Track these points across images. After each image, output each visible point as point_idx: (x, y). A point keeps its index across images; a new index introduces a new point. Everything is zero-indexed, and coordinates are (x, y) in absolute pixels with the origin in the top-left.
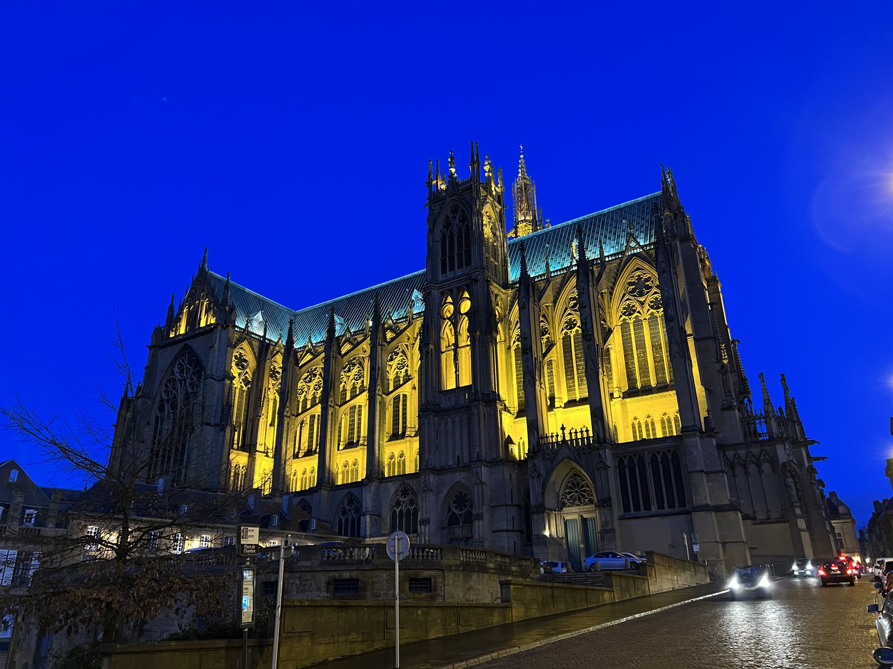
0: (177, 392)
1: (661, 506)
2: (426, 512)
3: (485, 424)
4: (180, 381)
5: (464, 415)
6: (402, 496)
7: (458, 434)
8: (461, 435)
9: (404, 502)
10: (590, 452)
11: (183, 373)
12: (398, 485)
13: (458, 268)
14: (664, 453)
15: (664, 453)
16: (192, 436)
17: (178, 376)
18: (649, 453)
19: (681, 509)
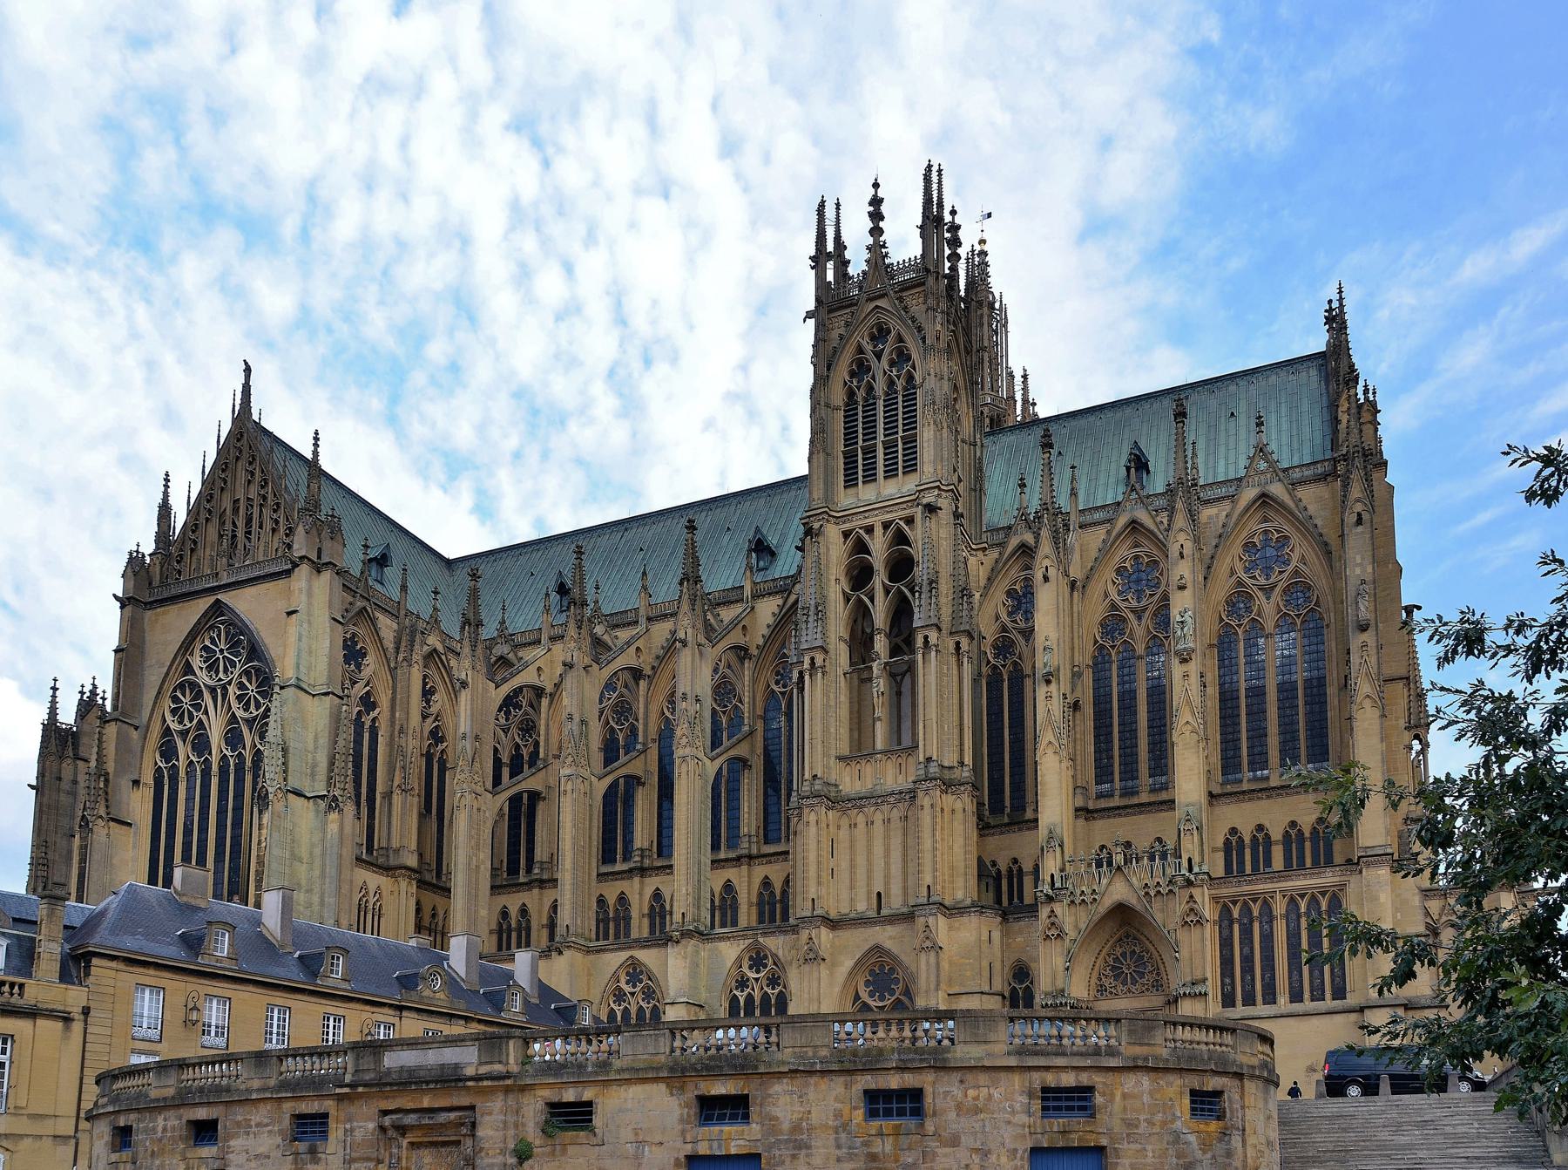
0: (206, 712)
1: (1296, 997)
3: (942, 829)
4: (213, 690)
5: (895, 809)
7: (878, 849)
10: (1171, 891)
11: (217, 672)
13: (885, 478)
14: (1313, 896)
15: (1313, 896)
16: (266, 817)
17: (203, 678)
18: (1284, 896)
19: (1338, 1004)
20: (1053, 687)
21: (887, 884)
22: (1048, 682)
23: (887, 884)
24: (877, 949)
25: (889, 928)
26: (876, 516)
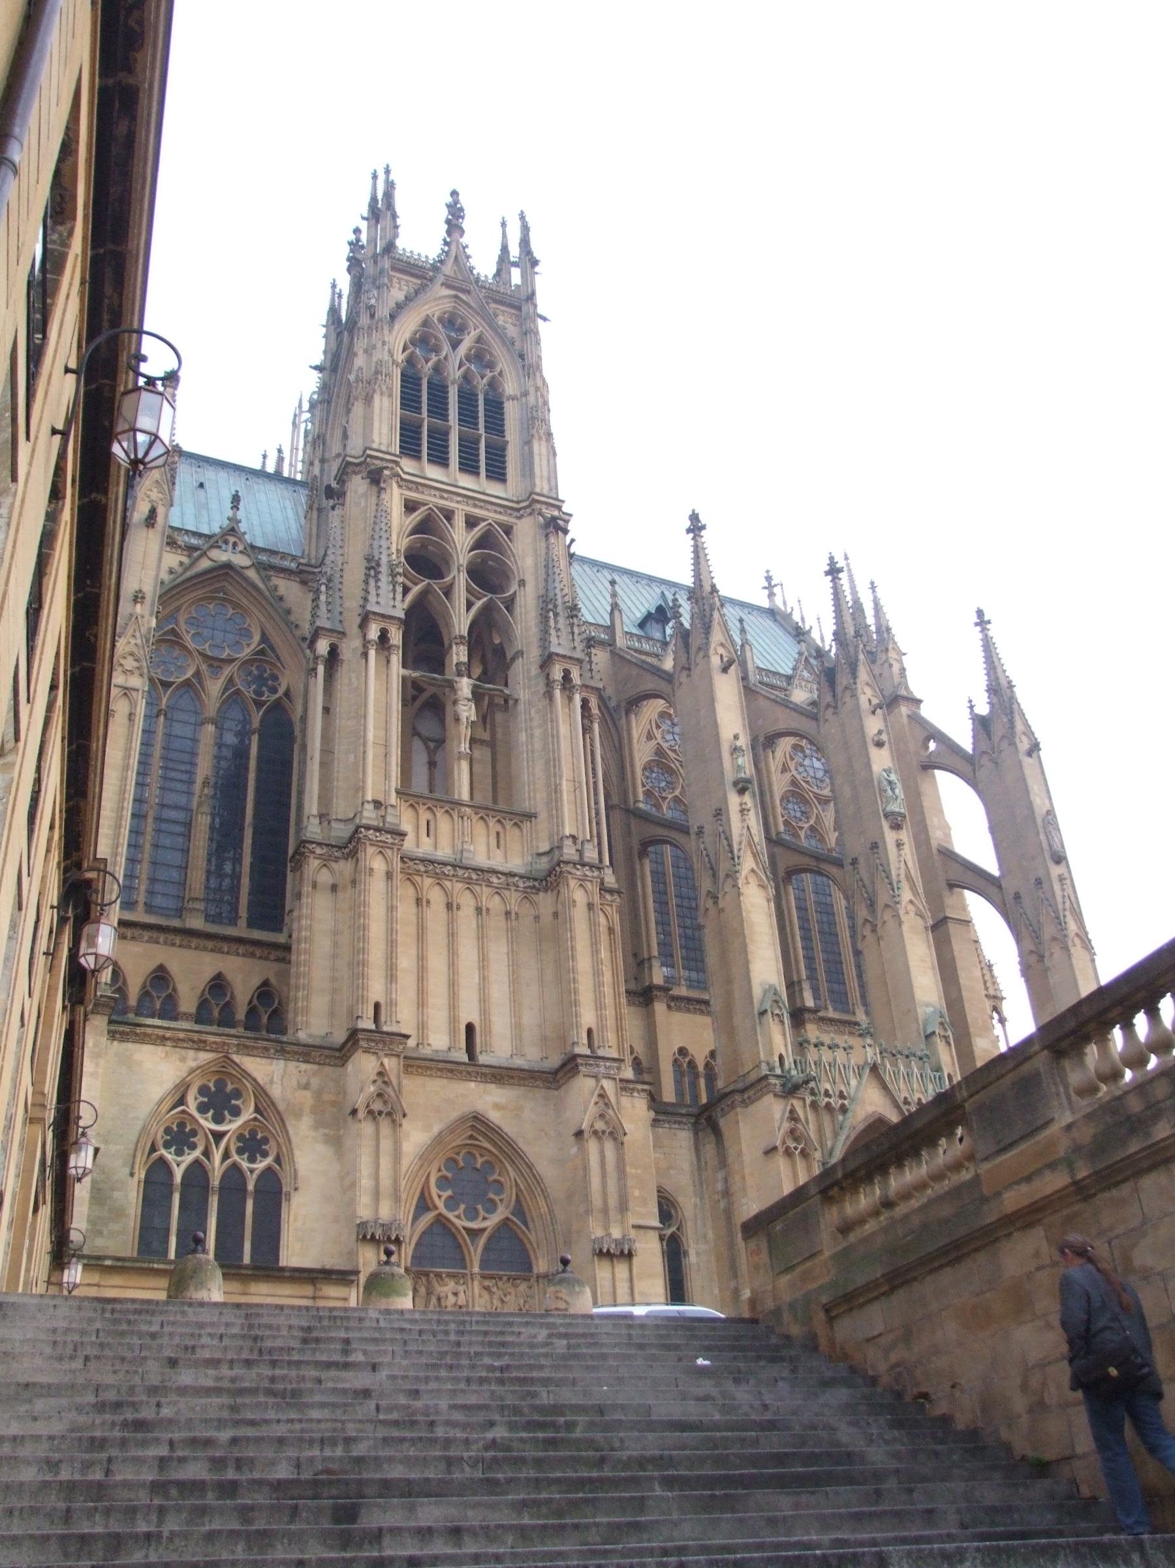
2: (376, 1195)
6: (202, 1109)
8: (452, 965)
9: (218, 1136)
12: (194, 1064)
20: (747, 798)
21: (485, 1012)
22: (742, 792)
23: (485, 1012)
24: (477, 1124)
25: (492, 1087)
26: (458, 502)
